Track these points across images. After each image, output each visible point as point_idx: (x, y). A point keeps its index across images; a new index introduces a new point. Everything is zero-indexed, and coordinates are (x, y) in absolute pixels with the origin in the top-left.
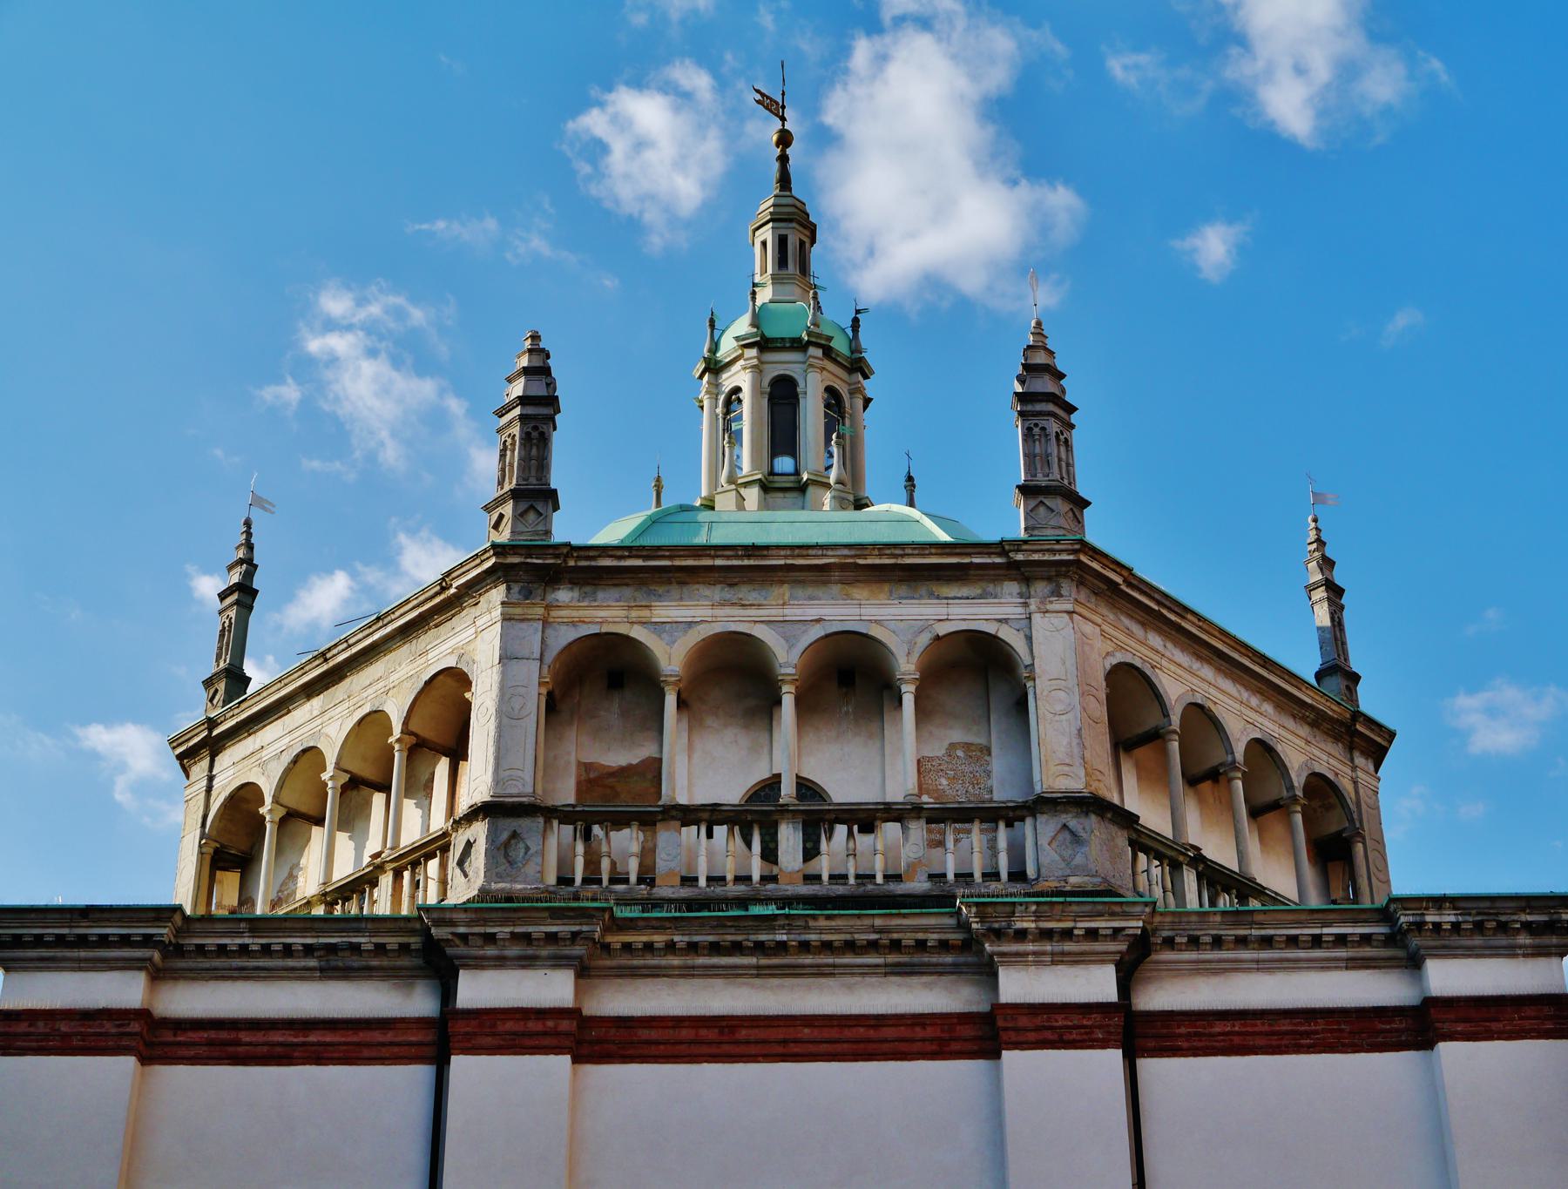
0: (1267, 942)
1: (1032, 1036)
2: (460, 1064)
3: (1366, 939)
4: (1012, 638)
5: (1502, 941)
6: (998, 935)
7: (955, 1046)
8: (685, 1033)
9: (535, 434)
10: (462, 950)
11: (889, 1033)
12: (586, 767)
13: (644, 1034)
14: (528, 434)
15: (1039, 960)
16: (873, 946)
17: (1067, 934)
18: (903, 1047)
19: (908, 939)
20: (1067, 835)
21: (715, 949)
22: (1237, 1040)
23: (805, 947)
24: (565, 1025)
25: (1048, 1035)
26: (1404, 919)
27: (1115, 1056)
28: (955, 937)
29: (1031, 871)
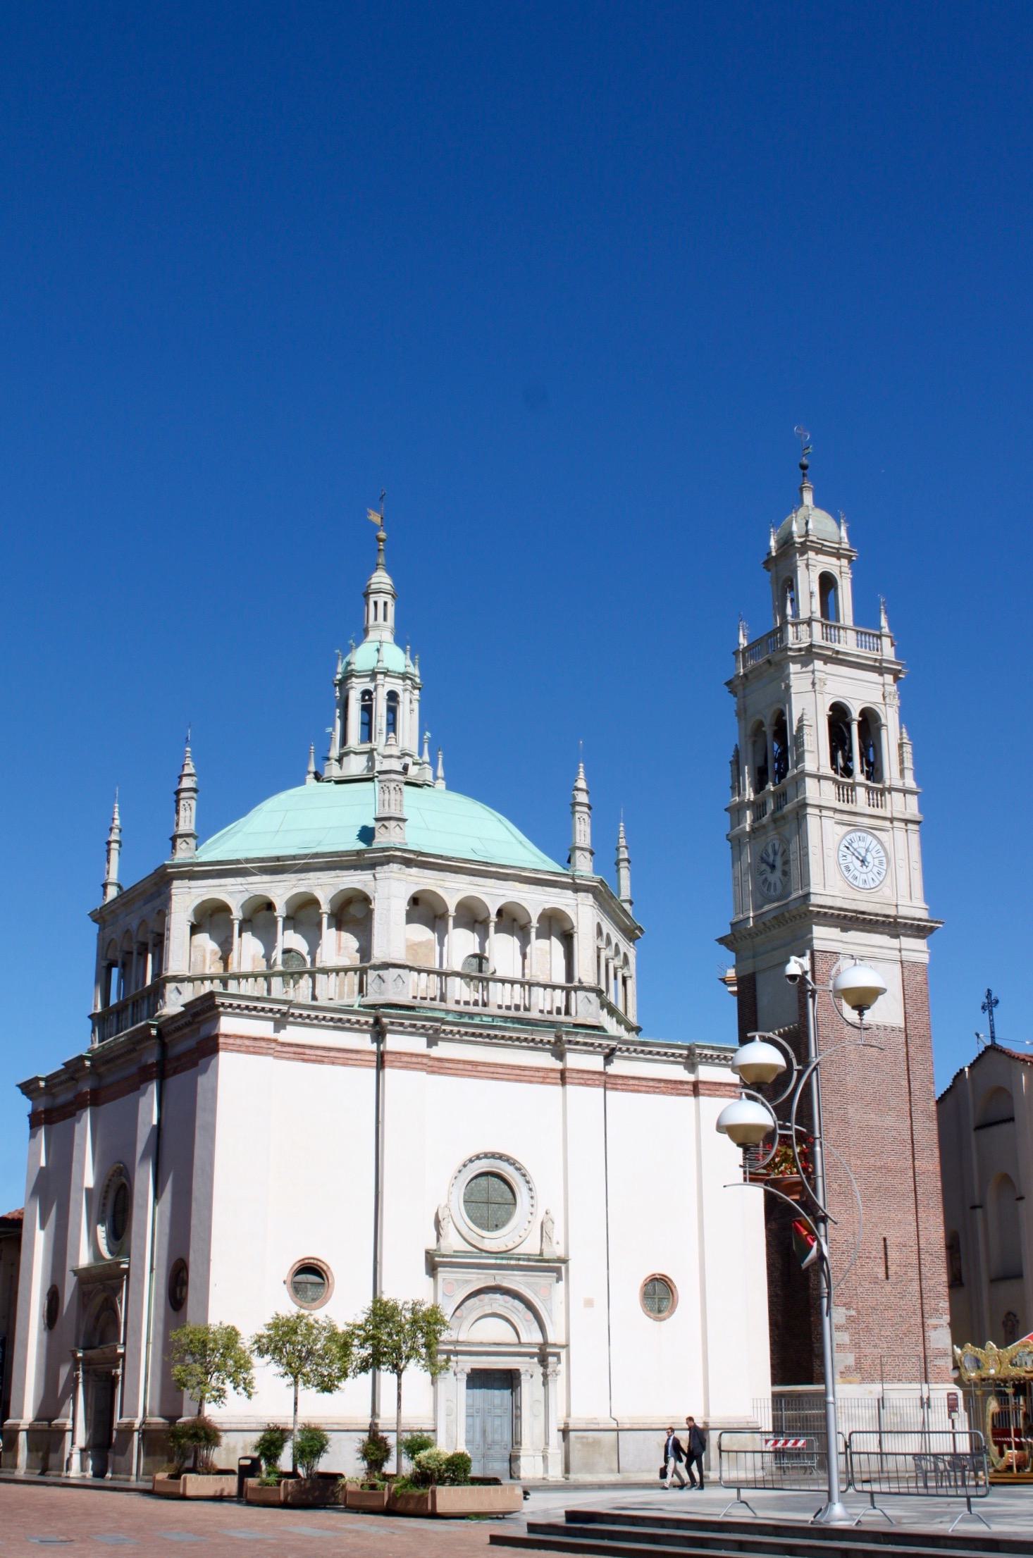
0: (650, 1053)
1: (576, 1081)
2: (388, 1072)
3: (681, 1055)
4: (570, 912)
5: (723, 1062)
6: (570, 1042)
7: (548, 1080)
8: (461, 1066)
9: (397, 788)
10: (390, 1027)
11: (527, 1073)
12: (407, 940)
13: (447, 1065)
14: (395, 788)
15: (580, 1051)
16: (526, 1040)
17: (592, 1045)
18: (532, 1079)
19: (538, 1038)
20: (586, 1000)
21: (473, 1035)
22: (636, 1087)
23: (503, 1038)
24: (425, 1061)
25: (582, 1081)
26: (698, 1051)
27: (602, 1090)
28: (553, 1040)
29: (573, 1011)
